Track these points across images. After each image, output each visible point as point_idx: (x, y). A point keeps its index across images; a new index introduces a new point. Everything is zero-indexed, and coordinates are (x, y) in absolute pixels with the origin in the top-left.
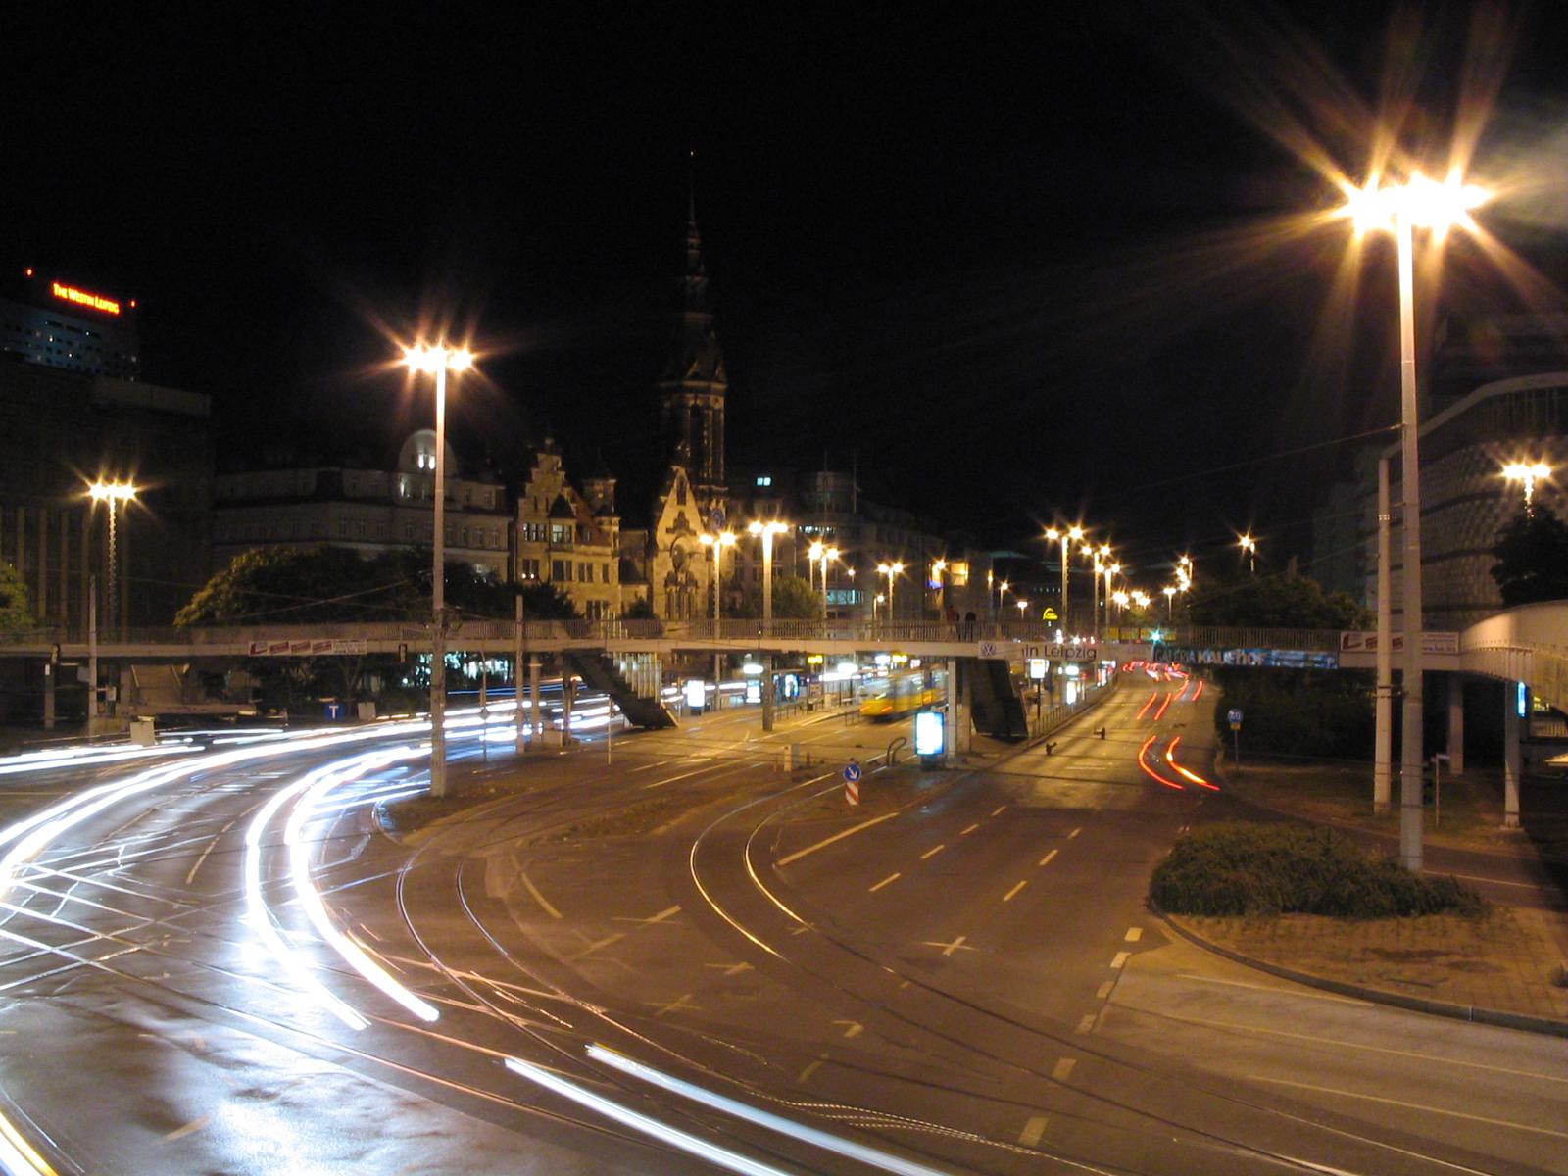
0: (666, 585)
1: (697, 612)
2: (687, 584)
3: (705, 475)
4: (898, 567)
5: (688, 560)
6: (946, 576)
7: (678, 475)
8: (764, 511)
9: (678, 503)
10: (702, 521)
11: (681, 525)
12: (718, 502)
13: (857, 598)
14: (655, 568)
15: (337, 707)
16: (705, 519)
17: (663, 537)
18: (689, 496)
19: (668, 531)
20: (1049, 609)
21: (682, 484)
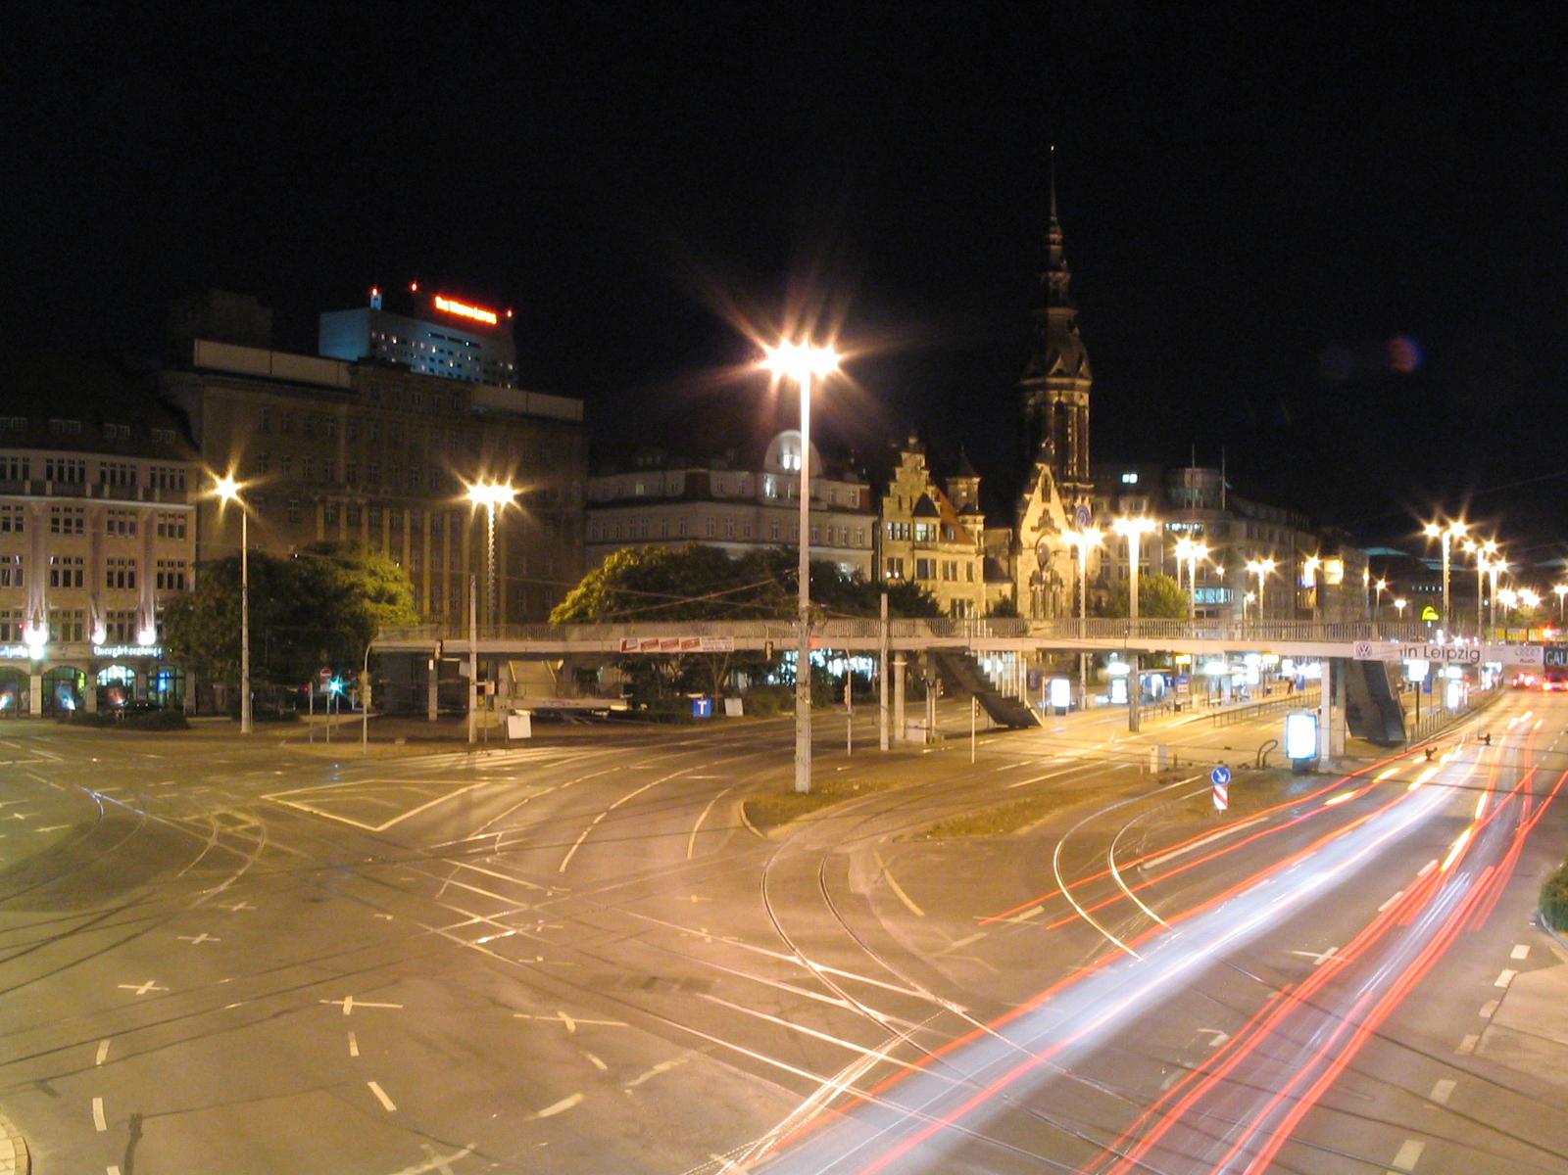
0: (1031, 584)
3: (1070, 473)
5: (1052, 559)
6: (1320, 575)
7: (1043, 473)
9: (1043, 500)
10: (1067, 519)
11: (1046, 522)
12: (1083, 499)
14: (1020, 568)
15: (705, 703)
16: (1070, 517)
17: (1027, 535)
18: (1054, 494)
19: (1033, 529)
21: (1046, 481)
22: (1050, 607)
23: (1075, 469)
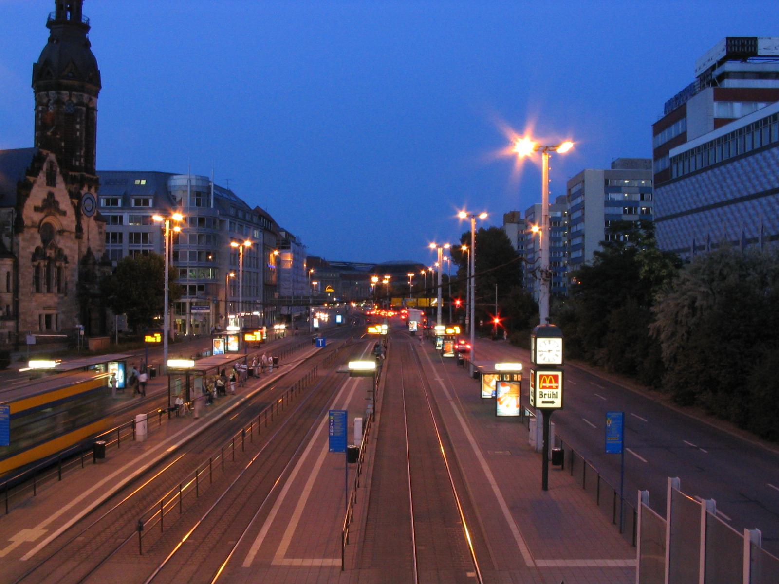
0: (34, 260)
1: (66, 284)
2: (55, 260)
3: (77, 164)
5: (58, 238)
6: (278, 261)
9: (48, 185)
10: (72, 203)
11: (50, 204)
12: (90, 188)
13: (214, 275)
14: (22, 244)
15: (322, 340)
16: (76, 201)
17: (30, 215)
18: (59, 179)
19: (36, 209)
21: (51, 167)
22: (54, 282)
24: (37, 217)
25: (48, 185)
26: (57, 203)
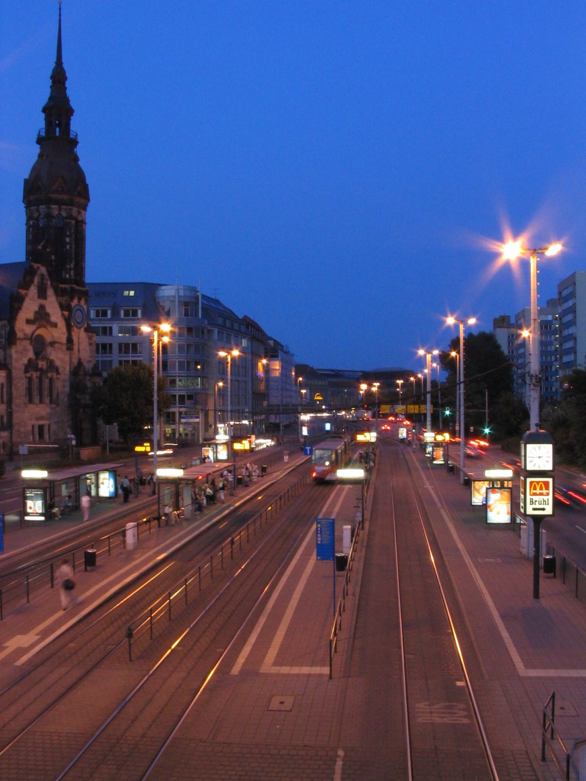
0: (26, 371)
1: (58, 395)
2: (47, 371)
3: (67, 276)
4: (402, 381)
5: (49, 349)
6: (267, 369)
7: (39, 273)
8: (166, 317)
9: (39, 297)
10: (63, 315)
11: (41, 317)
12: (79, 299)
16: (66, 313)
17: (22, 327)
18: (50, 292)
19: (28, 322)
20: (318, 394)
21: (42, 279)
22: (46, 393)
23: (72, 272)
24: (29, 329)
25: (39, 297)
26: (48, 315)
